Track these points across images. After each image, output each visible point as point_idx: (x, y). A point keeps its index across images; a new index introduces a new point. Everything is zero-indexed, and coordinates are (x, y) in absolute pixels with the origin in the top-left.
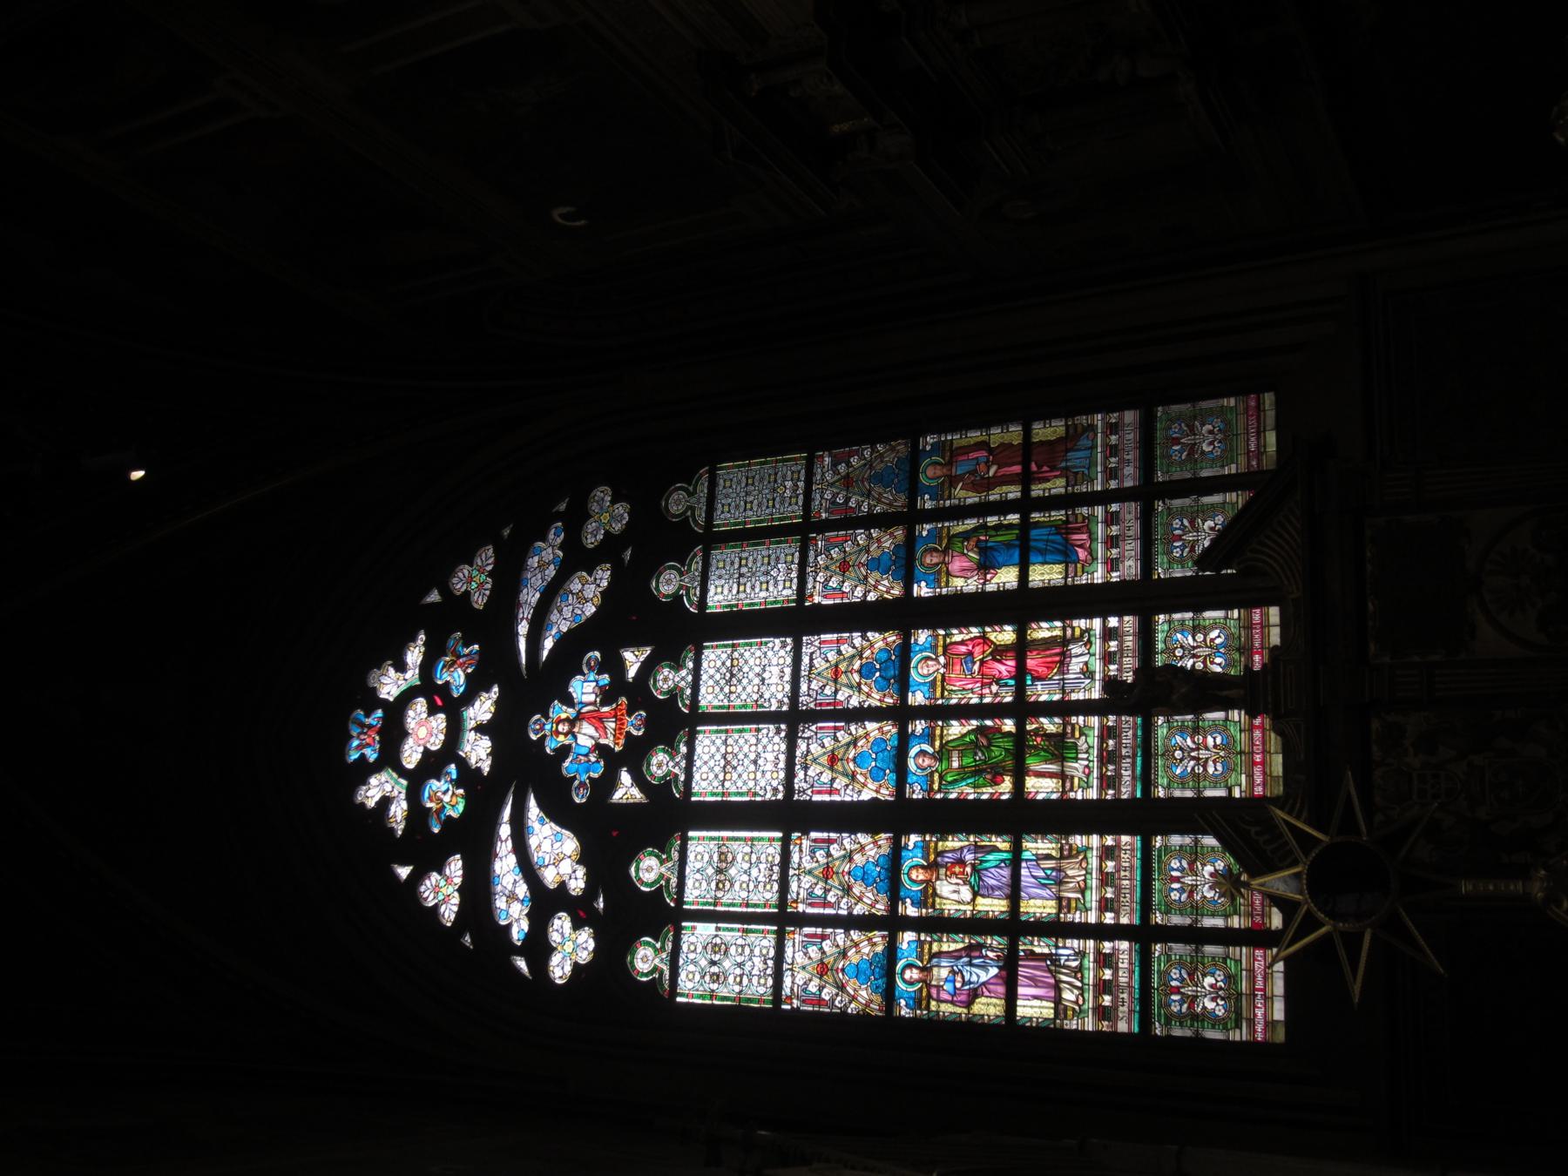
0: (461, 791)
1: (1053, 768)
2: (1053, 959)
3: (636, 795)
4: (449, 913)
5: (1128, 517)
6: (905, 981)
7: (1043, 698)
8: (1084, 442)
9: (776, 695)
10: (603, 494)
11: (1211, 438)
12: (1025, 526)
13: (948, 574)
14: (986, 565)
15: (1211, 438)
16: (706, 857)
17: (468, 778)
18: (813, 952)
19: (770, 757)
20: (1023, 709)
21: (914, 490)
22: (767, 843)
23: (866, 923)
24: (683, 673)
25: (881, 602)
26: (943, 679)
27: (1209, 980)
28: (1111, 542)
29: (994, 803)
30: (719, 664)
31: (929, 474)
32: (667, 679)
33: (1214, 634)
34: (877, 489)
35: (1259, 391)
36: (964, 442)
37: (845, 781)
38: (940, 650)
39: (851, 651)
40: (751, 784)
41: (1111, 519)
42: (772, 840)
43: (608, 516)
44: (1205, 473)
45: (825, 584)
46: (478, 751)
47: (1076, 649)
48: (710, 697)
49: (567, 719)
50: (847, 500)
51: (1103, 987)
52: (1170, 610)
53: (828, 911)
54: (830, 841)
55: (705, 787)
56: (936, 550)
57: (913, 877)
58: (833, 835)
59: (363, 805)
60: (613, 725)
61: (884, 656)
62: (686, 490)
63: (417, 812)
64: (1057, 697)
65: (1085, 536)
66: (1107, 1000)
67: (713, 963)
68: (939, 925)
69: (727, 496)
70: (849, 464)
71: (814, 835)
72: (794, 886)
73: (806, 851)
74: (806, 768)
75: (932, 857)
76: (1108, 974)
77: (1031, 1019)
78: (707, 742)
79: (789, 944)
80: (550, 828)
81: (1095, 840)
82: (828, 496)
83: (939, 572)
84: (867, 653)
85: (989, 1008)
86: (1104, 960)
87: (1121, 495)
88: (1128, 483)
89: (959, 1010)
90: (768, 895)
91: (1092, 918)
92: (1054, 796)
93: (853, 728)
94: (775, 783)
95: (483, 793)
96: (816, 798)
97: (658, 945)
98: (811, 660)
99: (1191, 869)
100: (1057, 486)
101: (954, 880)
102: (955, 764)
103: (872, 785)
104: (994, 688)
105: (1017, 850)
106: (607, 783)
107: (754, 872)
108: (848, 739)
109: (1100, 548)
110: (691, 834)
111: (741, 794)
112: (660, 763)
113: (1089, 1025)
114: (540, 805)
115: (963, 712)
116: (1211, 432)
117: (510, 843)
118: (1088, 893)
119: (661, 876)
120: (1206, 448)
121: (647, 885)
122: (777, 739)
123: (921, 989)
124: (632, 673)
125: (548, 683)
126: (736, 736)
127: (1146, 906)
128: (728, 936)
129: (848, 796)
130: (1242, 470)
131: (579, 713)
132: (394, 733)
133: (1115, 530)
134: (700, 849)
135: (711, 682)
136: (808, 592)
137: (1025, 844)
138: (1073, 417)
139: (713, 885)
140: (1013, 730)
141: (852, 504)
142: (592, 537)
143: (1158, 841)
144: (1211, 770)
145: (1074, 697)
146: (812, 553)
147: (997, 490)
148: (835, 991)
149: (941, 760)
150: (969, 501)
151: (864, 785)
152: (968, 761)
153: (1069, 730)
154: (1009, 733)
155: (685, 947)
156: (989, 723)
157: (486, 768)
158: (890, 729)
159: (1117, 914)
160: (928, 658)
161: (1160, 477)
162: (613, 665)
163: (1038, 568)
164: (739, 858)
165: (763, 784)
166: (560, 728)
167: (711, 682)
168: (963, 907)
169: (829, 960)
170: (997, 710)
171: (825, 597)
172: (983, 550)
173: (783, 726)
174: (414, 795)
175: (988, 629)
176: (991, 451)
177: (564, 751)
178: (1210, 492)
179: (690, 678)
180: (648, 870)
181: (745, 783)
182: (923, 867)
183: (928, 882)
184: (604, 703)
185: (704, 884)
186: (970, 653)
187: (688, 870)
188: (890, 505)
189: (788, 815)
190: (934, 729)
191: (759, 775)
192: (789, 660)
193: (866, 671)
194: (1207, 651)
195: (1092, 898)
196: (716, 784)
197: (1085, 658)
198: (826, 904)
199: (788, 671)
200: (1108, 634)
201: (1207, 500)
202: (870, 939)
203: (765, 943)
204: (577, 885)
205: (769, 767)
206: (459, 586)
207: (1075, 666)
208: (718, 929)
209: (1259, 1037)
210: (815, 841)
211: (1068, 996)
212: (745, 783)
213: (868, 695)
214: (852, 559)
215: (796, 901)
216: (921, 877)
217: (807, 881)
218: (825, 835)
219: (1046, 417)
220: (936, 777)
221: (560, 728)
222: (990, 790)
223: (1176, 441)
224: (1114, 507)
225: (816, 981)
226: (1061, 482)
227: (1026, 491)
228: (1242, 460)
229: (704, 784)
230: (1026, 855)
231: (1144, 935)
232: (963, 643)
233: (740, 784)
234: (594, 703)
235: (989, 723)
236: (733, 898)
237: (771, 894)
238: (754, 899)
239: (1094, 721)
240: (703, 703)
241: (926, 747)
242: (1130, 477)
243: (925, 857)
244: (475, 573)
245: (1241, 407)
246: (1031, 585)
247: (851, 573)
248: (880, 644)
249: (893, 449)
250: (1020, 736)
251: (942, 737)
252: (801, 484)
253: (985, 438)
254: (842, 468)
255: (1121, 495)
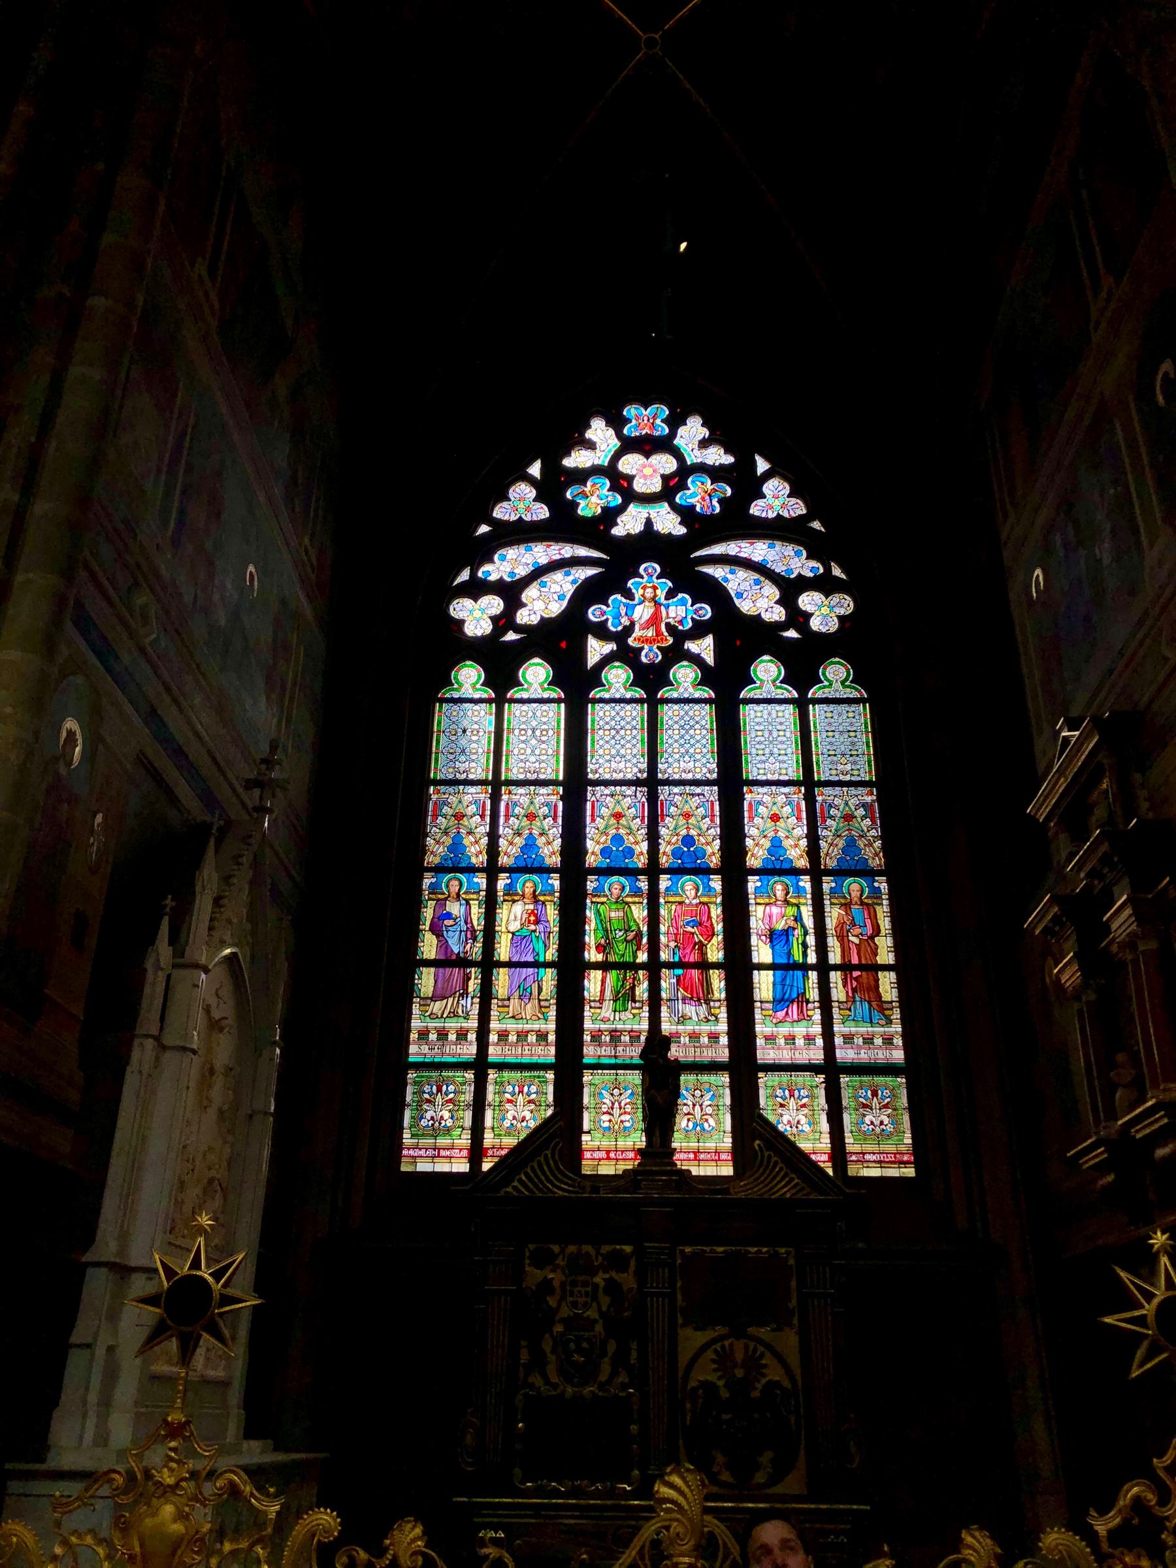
0: (599, 511)
1: (608, 994)
2: (465, 994)
3: (592, 659)
4: (501, 512)
5: (812, 1052)
6: (450, 880)
7: (663, 983)
8: (876, 1016)
9: (669, 768)
10: (844, 604)
11: (877, 1123)
12: (804, 967)
13: (767, 904)
14: (772, 936)
15: (877, 1123)
16: (545, 720)
17: (610, 515)
18: (472, 809)
19: (622, 765)
20: (654, 968)
21: (840, 873)
22: (555, 768)
23: (493, 850)
24: (691, 690)
25: (743, 852)
26: (680, 903)
27: (446, 1115)
28: (791, 1039)
29: (582, 946)
30: (697, 719)
31: (854, 886)
32: (684, 676)
33: (712, 1122)
34: (841, 843)
35: (917, 1164)
36: (880, 915)
37: (601, 827)
38: (705, 899)
39: (704, 827)
40: (601, 752)
41: (809, 1039)
42: (557, 771)
43: (824, 612)
44: (846, 1117)
45: (760, 803)
46: (630, 523)
47: (703, 1010)
48: (670, 713)
49: (655, 596)
50: (832, 817)
51: (443, 1034)
52: (732, 1086)
53: (502, 820)
54: (555, 819)
55: (598, 716)
56: (787, 893)
57: (527, 883)
58: (560, 820)
59: (589, 427)
60: (650, 634)
61: (699, 855)
62: (846, 679)
63: (581, 476)
64: (664, 995)
65: (795, 1017)
66: (433, 1037)
67: (464, 731)
68: (491, 905)
69: (840, 715)
70: (863, 818)
71: (560, 804)
72: (521, 790)
73: (550, 797)
74: (612, 796)
75: (542, 898)
76: (452, 1037)
77: (420, 978)
78: (635, 713)
79: (479, 788)
80: (569, 590)
81: (552, 1026)
82: (837, 801)
83: (769, 897)
84: (702, 840)
85: (429, 947)
86: (462, 1035)
87: (829, 1048)
88: (839, 1054)
89: (428, 923)
90: (515, 771)
91: (494, 1025)
92: (586, 993)
93: (644, 831)
94: (601, 771)
95: (594, 531)
96: (589, 805)
97: (478, 686)
98: (698, 795)
99: (530, 1102)
100: (838, 993)
101: (525, 916)
102: (613, 914)
103: (598, 849)
104: (672, 944)
105: (547, 965)
106: (601, 631)
107: (533, 759)
108: (634, 828)
109: (784, 1030)
110: (563, 705)
111: (593, 744)
112: (618, 678)
113: (416, 1024)
114: (588, 580)
115: (654, 919)
116: (882, 1123)
117: (558, 557)
118: (513, 1021)
119: (530, 685)
120: (867, 1119)
121: (524, 674)
122: (635, 770)
123: (443, 894)
124: (692, 646)
125: (686, 576)
126: (639, 737)
127: (501, 1067)
128: (484, 741)
129: (590, 830)
130: (849, 1148)
131: (660, 605)
132: (647, 446)
133: (800, 1042)
134: (551, 714)
135: (682, 713)
136: (754, 788)
137: (549, 970)
138: (900, 1007)
139: (523, 726)
140: (638, 961)
141: (829, 822)
142: (808, 601)
143: (550, 1076)
144: (606, 1117)
145: (664, 1009)
146: (786, 790)
147: (837, 944)
148: (443, 827)
149: (617, 902)
150: (828, 920)
151: (598, 843)
152: (615, 925)
153: (637, 1005)
154: (635, 957)
155: (477, 707)
156: (645, 940)
157: (618, 531)
158: (641, 861)
159: (497, 1044)
160: (697, 890)
161: (844, 1079)
162: (699, 630)
163: (771, 979)
164: (543, 746)
165: (601, 761)
166: (649, 590)
167: (682, 713)
168: (504, 924)
169: (465, 821)
170: (654, 947)
171: (750, 804)
172: (787, 933)
173: (645, 775)
174: (596, 470)
175: (720, 937)
176: (872, 938)
177: (629, 595)
178: (830, 1120)
179: (686, 695)
180: (536, 674)
181: (601, 747)
182: (535, 891)
183: (523, 896)
184: (668, 625)
185: (524, 719)
186: (701, 924)
187: (535, 705)
188: (827, 854)
189: (576, 784)
190: (641, 896)
191: (608, 757)
192: (698, 776)
193: (688, 840)
194: (698, 1116)
195: (511, 1026)
196: (601, 723)
197: (695, 1018)
198: (507, 817)
199: (690, 776)
200: (714, 1037)
201: (824, 1118)
202: (481, 852)
203: (480, 770)
204: (524, 617)
205: (614, 765)
206: (770, 487)
207: (690, 1010)
208: (490, 733)
209: (405, 1152)
210: (556, 806)
211: (437, 1007)
212: (601, 747)
213: (669, 843)
214: (781, 824)
215: (510, 793)
216: (527, 890)
217: (525, 801)
218: (560, 813)
219: (901, 985)
220: (604, 899)
221: (649, 590)
222: (593, 943)
223: (875, 1094)
224: (820, 1042)
225: (450, 811)
226: (843, 998)
227: (836, 968)
228: (857, 1148)
229: (601, 713)
230: (542, 970)
231: (480, 1066)
232: (709, 917)
233: (601, 742)
234: (668, 617)
235: (645, 940)
236: (513, 743)
237: (516, 774)
238: (513, 761)
239: (645, 1026)
240: (666, 707)
241: (627, 889)
242: (843, 1054)
243: (540, 894)
244: (781, 500)
245: (903, 1148)
246: (755, 972)
247: (770, 823)
248: (709, 850)
249: (876, 855)
250: (634, 967)
251: (634, 903)
252: (848, 778)
253: (883, 932)
254: (861, 812)
255: (829, 1048)
